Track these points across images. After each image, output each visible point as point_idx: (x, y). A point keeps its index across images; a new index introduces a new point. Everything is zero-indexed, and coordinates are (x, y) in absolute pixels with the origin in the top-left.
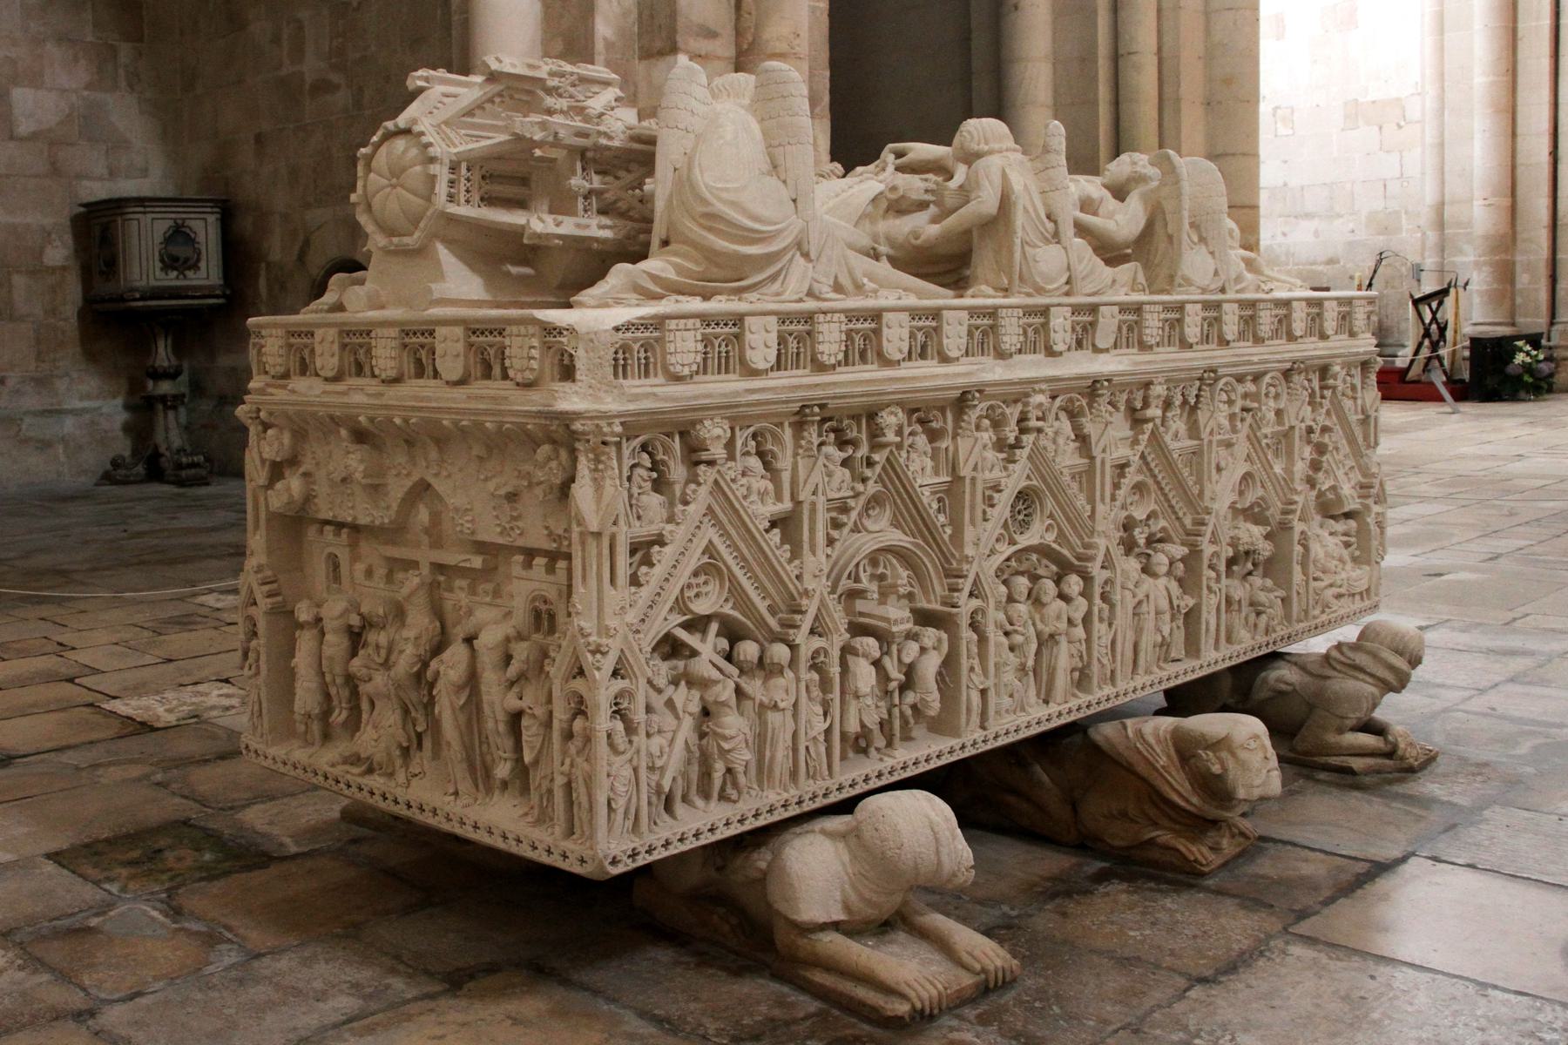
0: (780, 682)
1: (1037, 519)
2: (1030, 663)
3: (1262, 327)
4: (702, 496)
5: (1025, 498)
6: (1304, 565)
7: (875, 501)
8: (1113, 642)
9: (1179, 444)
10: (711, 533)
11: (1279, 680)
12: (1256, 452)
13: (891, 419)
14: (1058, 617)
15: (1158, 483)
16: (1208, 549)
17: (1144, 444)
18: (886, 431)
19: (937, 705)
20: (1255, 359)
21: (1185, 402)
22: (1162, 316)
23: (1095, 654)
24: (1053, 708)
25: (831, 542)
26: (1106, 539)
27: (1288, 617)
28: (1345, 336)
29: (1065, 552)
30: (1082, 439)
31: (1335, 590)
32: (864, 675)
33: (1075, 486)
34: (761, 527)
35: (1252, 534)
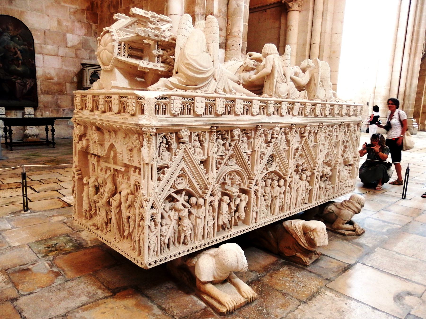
0: (201, 210)
1: (274, 163)
2: (269, 204)
3: (335, 112)
4: (181, 153)
5: (272, 157)
6: (338, 178)
7: (231, 157)
8: (291, 199)
9: (312, 144)
10: (183, 165)
11: (330, 209)
12: (330, 147)
13: (236, 132)
14: (277, 192)
15: (306, 154)
16: (316, 173)
17: (303, 143)
18: (235, 136)
19: (244, 216)
20: (333, 121)
21: (314, 132)
22: (311, 107)
23: (286, 202)
24: (274, 217)
25: (218, 168)
26: (291, 170)
27: (334, 192)
28: (355, 116)
29: (281, 173)
30: (287, 141)
32: (225, 207)
33: (284, 154)
34: (198, 163)
35: (327, 170)
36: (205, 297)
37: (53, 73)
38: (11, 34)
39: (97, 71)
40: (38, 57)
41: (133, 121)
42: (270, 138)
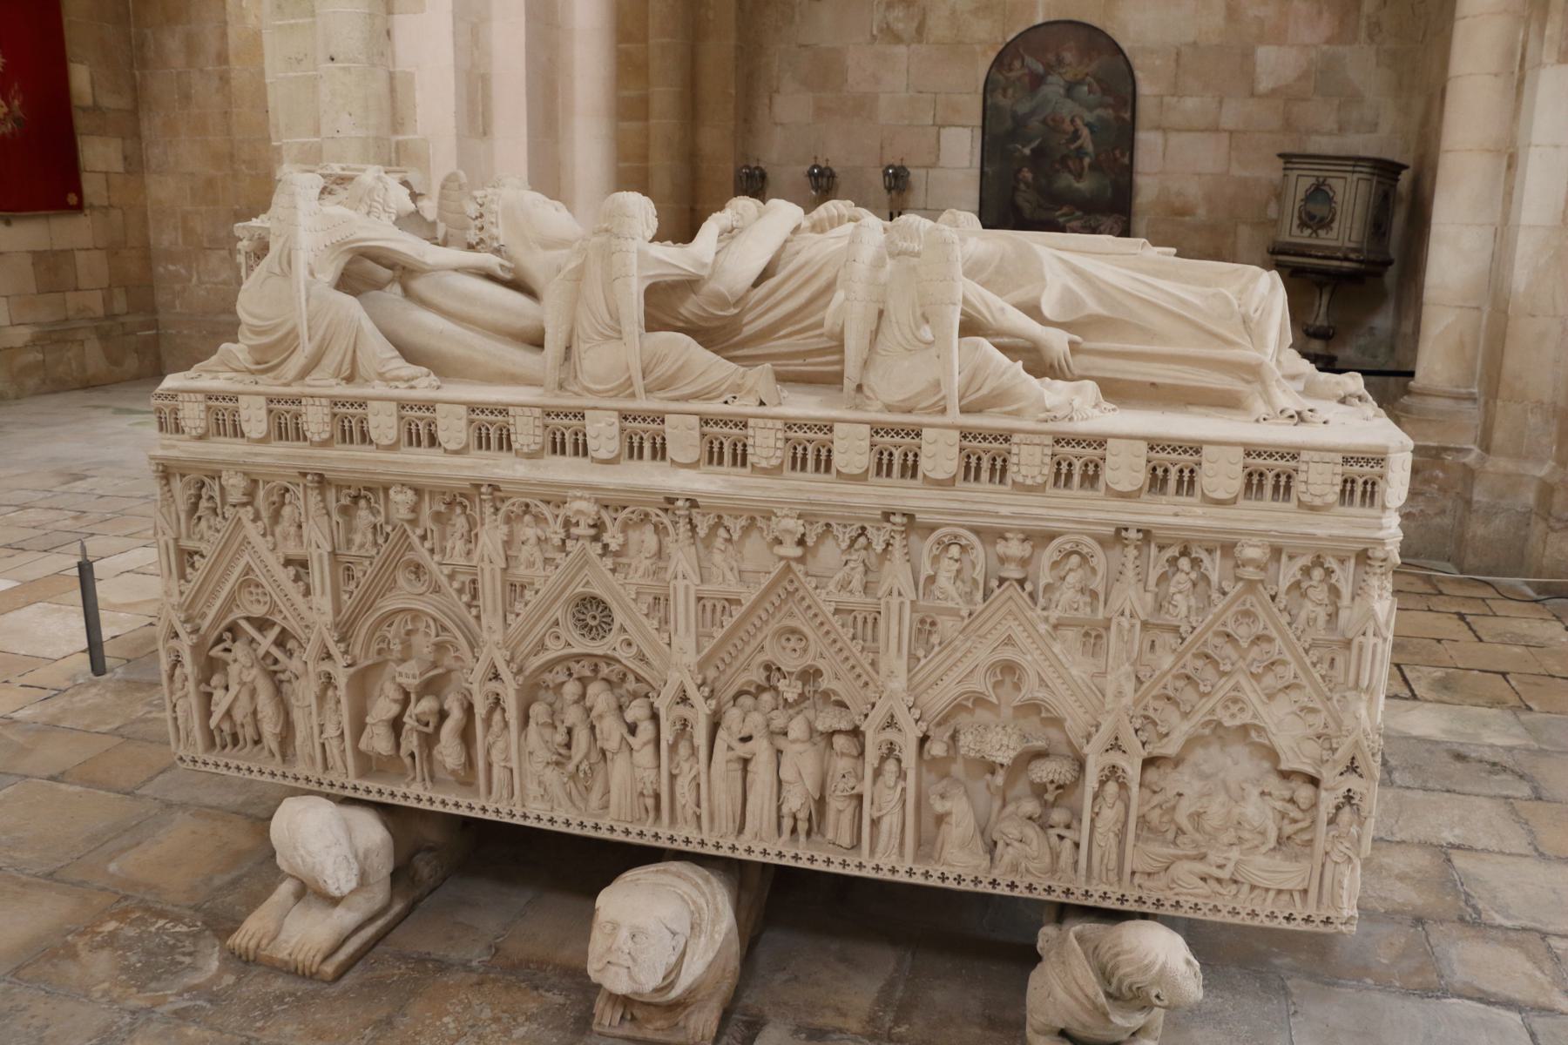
13: (401, 499)
20: (1004, 511)
24: (605, 823)
31: (1200, 867)
37: (1193, 190)
38: (1069, 77)
39: (1330, 181)
40: (1147, 140)
42: (563, 535)
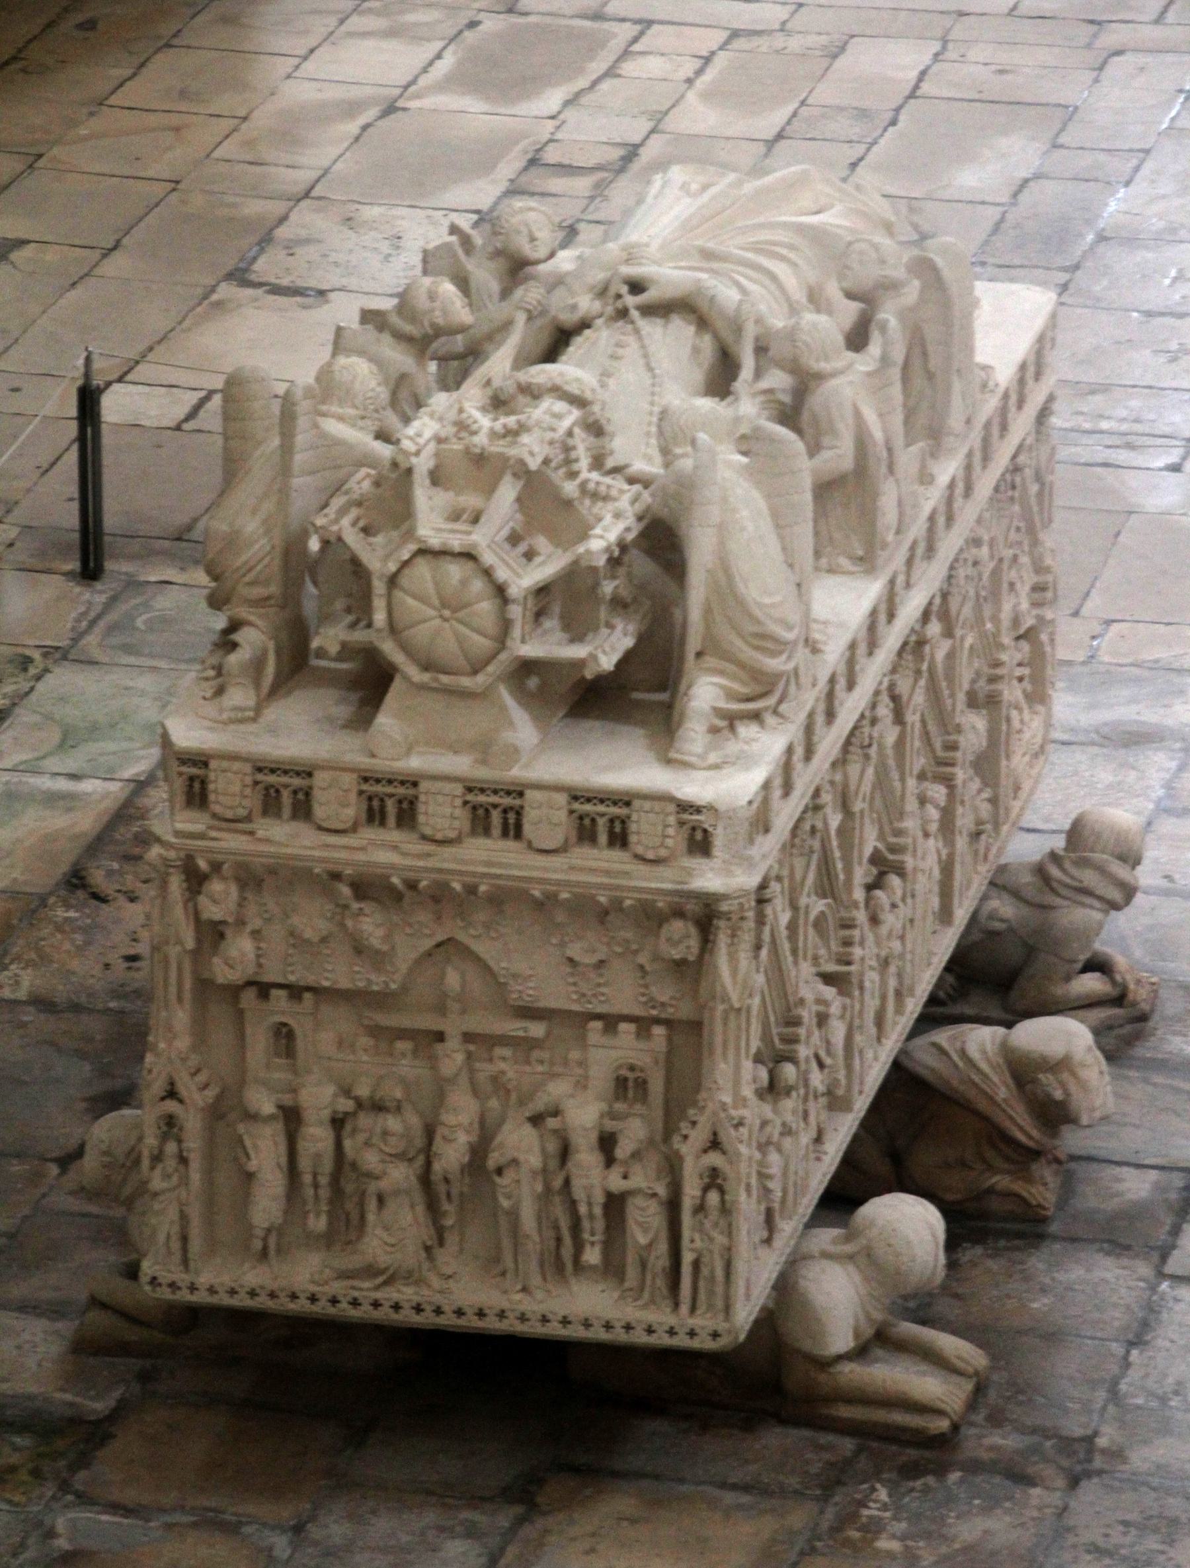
36: (845, 1412)
41: (660, 881)
